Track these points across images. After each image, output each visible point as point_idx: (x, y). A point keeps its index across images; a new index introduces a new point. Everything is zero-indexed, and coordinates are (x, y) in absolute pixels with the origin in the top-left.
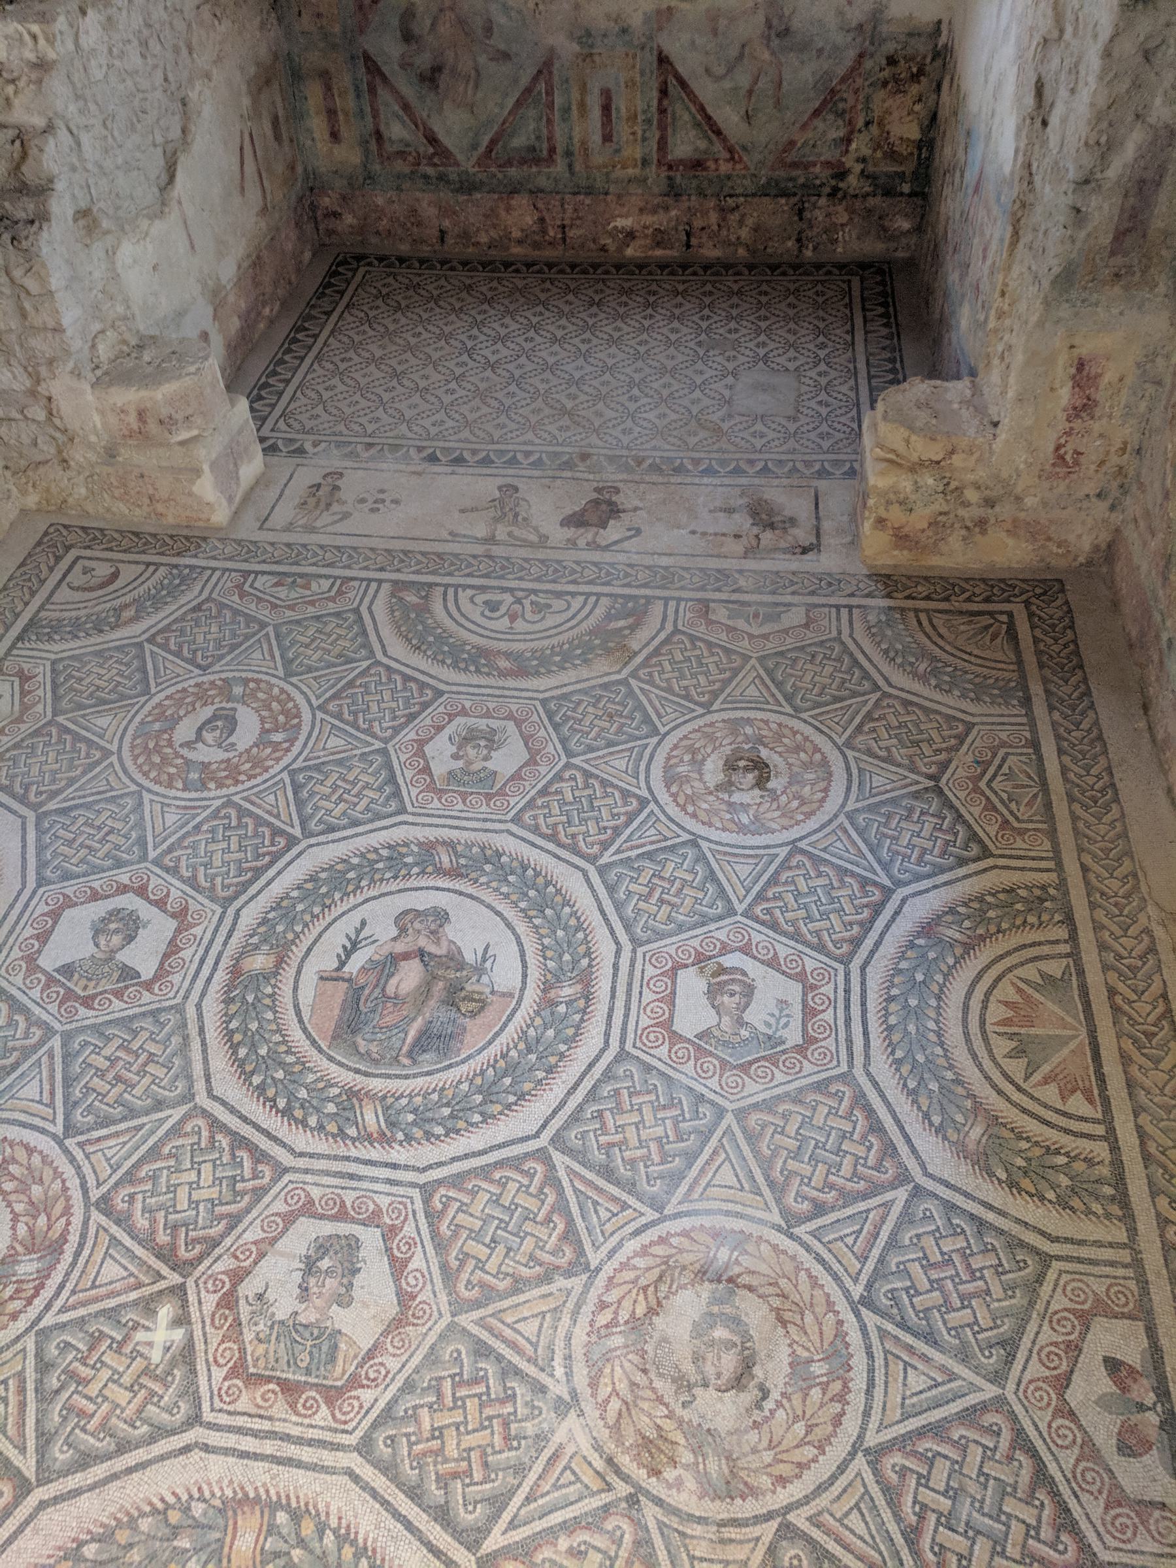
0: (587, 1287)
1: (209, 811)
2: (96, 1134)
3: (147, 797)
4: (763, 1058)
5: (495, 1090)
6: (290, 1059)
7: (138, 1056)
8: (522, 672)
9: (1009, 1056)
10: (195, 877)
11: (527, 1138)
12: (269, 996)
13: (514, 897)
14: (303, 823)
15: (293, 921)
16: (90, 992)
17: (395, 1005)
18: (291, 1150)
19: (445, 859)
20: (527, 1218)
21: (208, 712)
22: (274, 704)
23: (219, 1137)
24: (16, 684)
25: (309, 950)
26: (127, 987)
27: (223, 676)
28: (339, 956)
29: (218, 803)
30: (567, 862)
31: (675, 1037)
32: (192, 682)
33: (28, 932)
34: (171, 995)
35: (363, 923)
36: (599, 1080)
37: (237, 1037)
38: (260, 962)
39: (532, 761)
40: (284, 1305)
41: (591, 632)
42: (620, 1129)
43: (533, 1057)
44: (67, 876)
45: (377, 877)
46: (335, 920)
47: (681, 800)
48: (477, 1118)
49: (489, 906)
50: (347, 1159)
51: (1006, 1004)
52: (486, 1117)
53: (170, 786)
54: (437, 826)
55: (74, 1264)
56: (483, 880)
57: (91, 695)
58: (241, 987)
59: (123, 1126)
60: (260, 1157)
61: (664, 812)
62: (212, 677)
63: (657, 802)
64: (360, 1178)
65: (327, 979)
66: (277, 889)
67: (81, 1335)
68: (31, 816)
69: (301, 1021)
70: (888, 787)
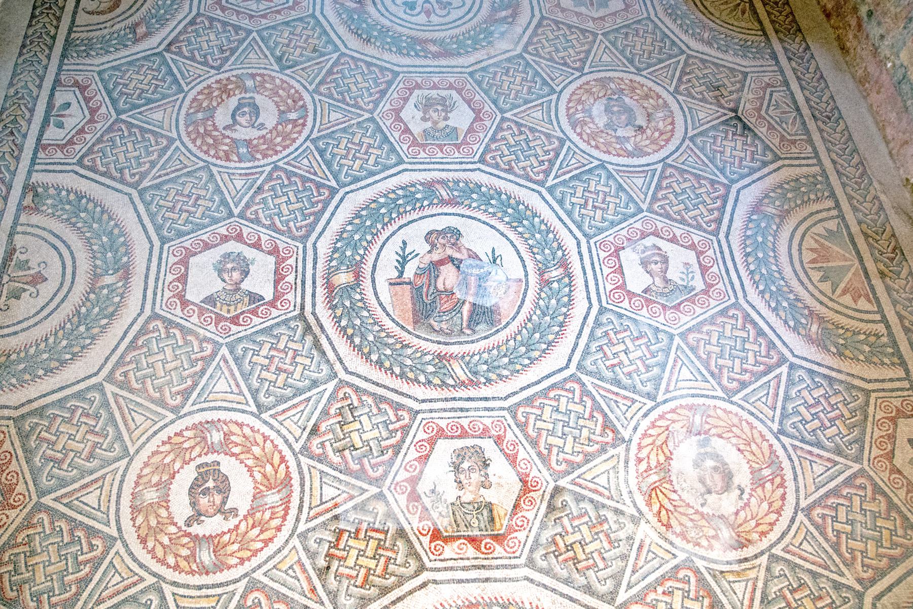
0: (628, 450)
1: (264, 175)
2: (280, 408)
3: (215, 170)
4: (686, 300)
5: (531, 342)
6: (391, 341)
7: (287, 354)
8: (447, 54)
9: (820, 281)
10: (274, 224)
11: (561, 370)
12: (360, 301)
13: (499, 215)
14: (335, 178)
15: (355, 248)
16: (232, 314)
18: (416, 399)
19: (444, 193)
20: (579, 418)
21: (233, 102)
22: (281, 92)
23: (364, 398)
24: (77, 92)
25: (374, 266)
26: (258, 307)
27: (234, 73)
28: (396, 267)
29: (268, 168)
30: (526, 187)
31: (631, 295)
32: (213, 80)
33: (170, 278)
34: (292, 308)
35: (404, 243)
36: (593, 328)
37: (350, 331)
38: (343, 278)
39: (478, 118)
40: (451, 493)
41: (485, 22)
42: (615, 355)
43: (548, 318)
44: (180, 234)
45: (401, 210)
46: (384, 244)
47: (585, 137)
48: (527, 362)
49: (484, 223)
50: (454, 399)
51: (811, 250)
52: (532, 361)
53: (228, 159)
54: (429, 170)
55: (303, 491)
56: (474, 205)
57: (139, 96)
59: (296, 400)
60: (398, 407)
61: (577, 146)
62: (226, 75)
63: (570, 140)
64: (467, 410)
65: (394, 284)
66: (335, 226)
67: (328, 532)
68: (135, 194)
69: (388, 315)
70: (709, 119)
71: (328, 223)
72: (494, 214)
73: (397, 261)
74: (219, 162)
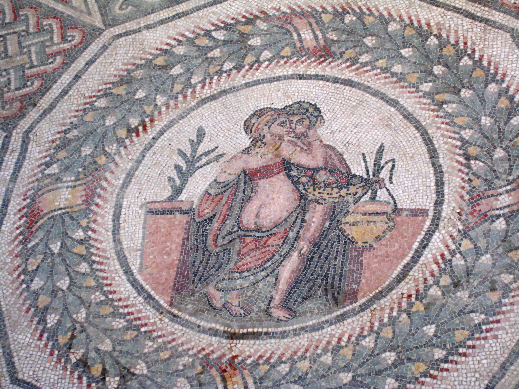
6: (119, 323)
12: (81, 242)
17: (257, 239)
19: (307, 36)
25: (130, 176)
30: (487, 21)
35: (201, 134)
37: (43, 300)
49: (376, 94)
56: (364, 58)
58: (41, 234)
69: (128, 272)
71: (65, 92)
72: (401, 78)
73: (178, 168)
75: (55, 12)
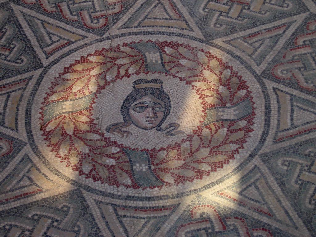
27: (128, 40)
74: (98, 185)
75: (262, 224)
